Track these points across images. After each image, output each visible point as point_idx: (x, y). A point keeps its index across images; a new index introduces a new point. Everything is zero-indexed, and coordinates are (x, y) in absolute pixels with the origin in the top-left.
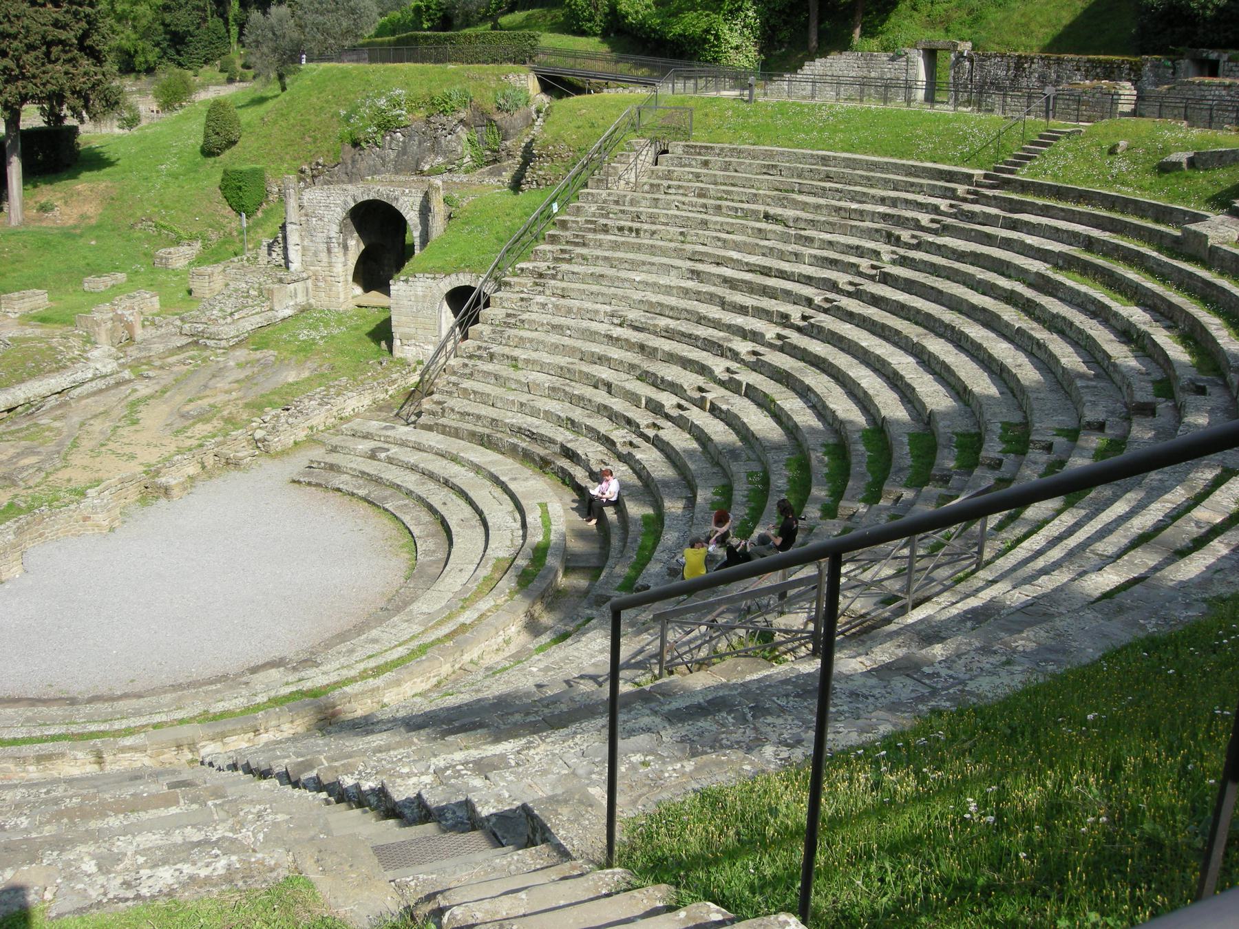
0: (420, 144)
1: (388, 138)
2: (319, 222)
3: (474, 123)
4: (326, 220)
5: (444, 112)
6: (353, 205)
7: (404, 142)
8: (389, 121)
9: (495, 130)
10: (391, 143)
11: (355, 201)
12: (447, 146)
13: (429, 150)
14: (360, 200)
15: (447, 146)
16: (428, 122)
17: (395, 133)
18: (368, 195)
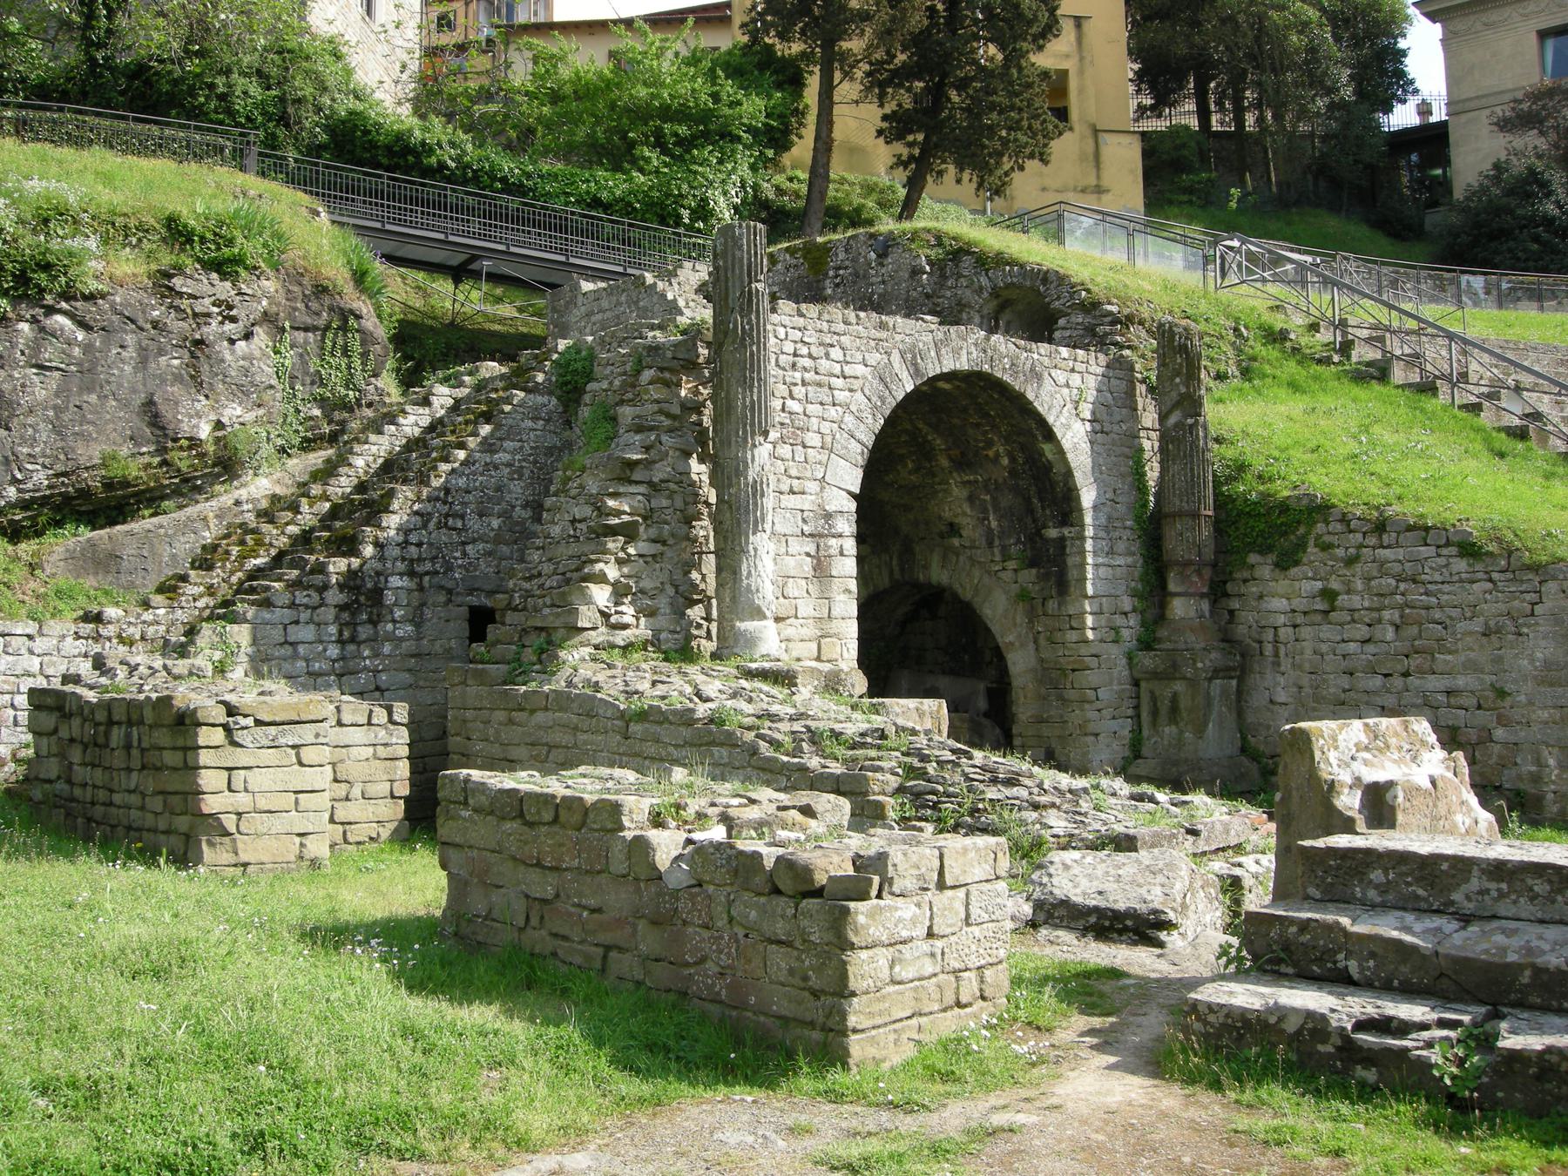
0: (143, 361)
1: (24, 327)
2: (785, 451)
3: (291, 317)
4: (813, 439)
5: (223, 267)
6: (910, 387)
7: (87, 348)
8: (47, 267)
9: (356, 346)
10: (36, 346)
11: (916, 371)
12: (246, 372)
13: (178, 378)
14: (932, 370)
15: (246, 372)
16: (163, 283)
17: (51, 311)
18: (956, 352)
